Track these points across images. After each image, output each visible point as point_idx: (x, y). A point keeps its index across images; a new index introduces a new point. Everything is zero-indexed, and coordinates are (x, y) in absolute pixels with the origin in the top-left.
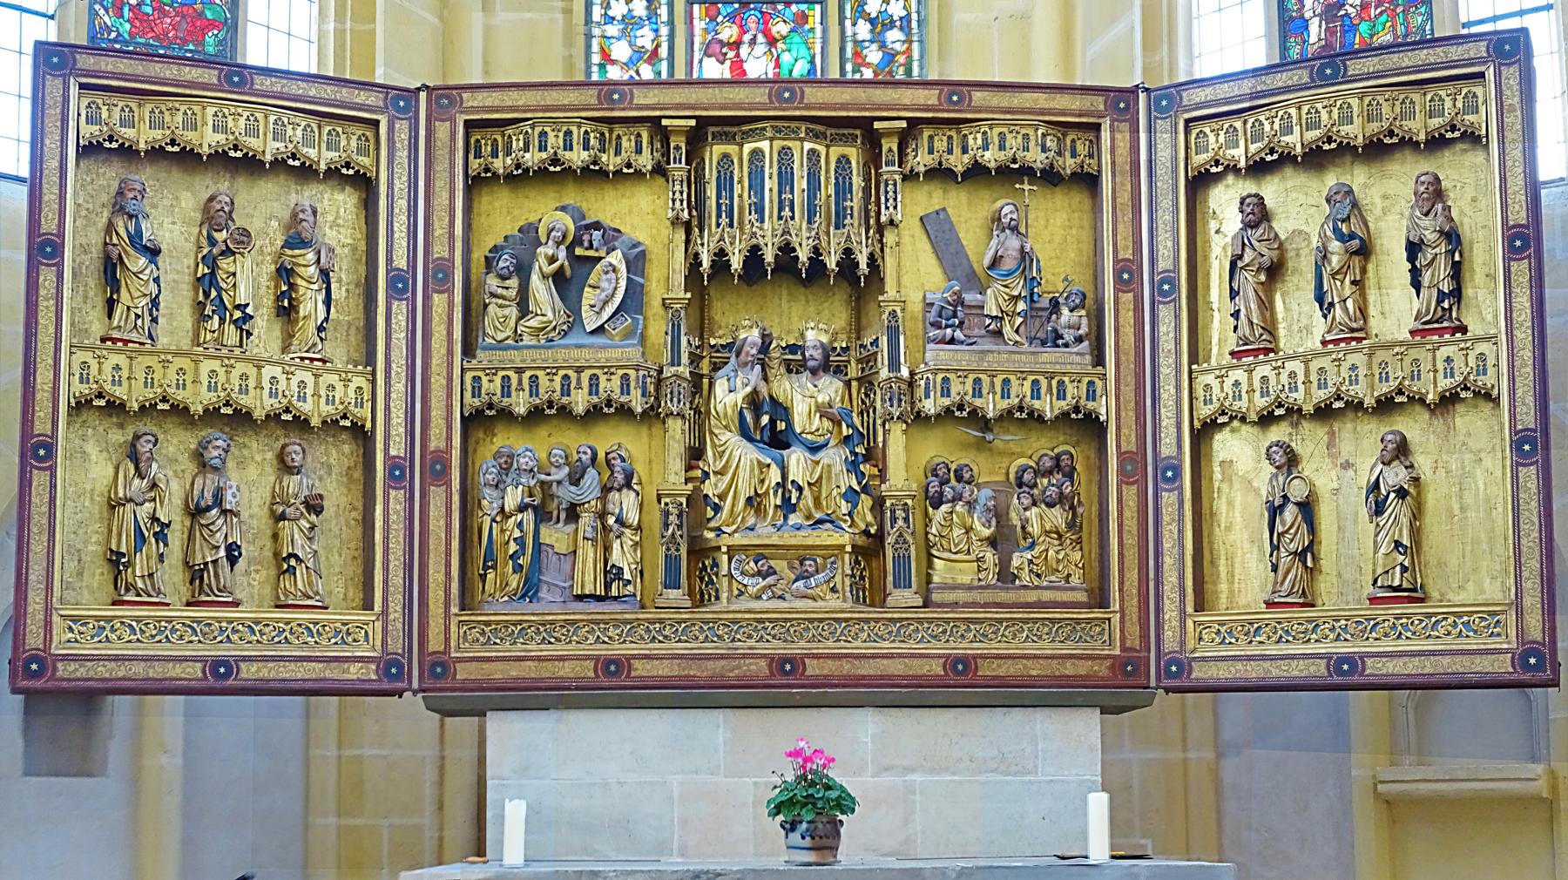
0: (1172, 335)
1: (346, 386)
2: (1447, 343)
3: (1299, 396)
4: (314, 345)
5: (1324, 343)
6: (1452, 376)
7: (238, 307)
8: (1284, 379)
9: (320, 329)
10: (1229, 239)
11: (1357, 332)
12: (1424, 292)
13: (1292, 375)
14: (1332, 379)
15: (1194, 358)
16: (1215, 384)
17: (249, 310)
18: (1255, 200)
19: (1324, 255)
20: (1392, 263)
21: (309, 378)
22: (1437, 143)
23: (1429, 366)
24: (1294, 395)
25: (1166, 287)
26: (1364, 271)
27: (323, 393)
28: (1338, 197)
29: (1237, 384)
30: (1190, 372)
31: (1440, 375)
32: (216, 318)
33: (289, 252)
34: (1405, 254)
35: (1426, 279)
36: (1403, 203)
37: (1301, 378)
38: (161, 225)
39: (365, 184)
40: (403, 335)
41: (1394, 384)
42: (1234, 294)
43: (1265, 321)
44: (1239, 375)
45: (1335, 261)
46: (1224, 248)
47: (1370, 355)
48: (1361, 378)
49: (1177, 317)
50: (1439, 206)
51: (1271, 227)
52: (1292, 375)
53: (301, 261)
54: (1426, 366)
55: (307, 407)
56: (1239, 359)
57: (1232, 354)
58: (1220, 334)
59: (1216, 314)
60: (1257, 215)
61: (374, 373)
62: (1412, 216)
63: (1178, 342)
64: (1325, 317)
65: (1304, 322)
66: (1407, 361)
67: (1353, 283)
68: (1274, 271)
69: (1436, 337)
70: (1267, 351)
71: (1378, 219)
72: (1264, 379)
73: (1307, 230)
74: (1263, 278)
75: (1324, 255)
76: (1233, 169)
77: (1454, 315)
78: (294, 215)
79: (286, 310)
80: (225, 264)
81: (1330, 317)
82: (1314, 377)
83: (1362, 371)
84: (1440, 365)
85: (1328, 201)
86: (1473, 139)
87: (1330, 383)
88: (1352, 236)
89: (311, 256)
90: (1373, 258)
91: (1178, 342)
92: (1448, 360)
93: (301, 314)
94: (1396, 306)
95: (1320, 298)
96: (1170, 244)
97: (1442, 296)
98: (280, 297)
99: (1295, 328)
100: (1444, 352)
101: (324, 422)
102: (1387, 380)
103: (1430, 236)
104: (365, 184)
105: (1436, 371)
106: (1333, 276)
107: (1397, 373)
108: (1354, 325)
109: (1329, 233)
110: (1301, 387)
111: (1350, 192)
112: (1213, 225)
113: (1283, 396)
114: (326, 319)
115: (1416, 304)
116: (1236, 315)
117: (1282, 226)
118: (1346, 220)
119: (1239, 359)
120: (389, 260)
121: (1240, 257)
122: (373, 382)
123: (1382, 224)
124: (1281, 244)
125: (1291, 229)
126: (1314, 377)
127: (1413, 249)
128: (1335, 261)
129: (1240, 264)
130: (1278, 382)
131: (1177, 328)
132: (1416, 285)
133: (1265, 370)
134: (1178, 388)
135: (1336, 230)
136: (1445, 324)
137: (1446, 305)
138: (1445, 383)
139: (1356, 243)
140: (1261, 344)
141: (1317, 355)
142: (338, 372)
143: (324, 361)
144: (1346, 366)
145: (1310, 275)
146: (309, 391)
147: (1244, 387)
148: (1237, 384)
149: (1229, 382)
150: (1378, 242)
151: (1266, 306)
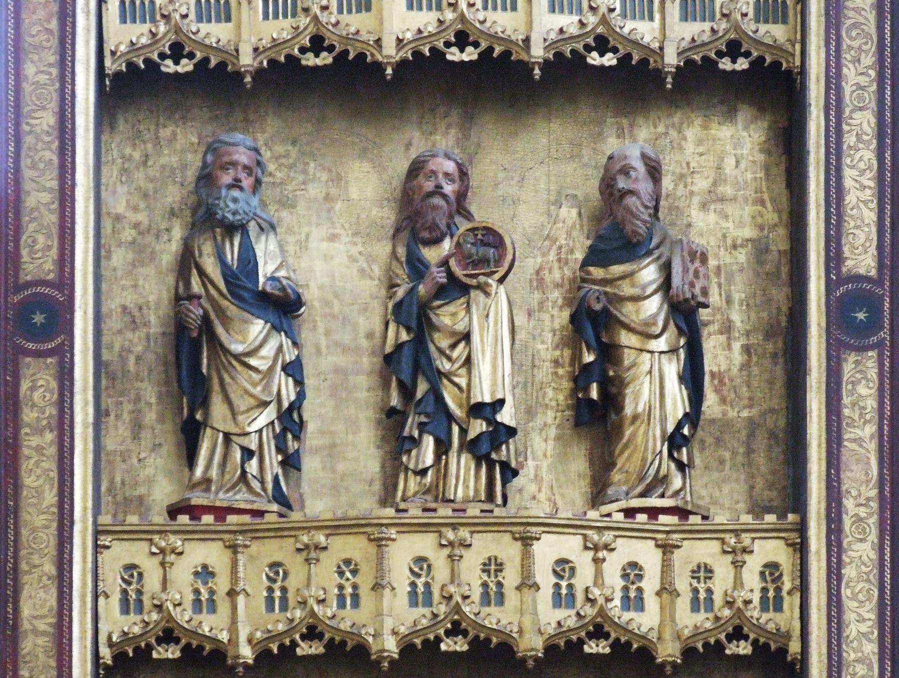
1: (738, 565)
4: (661, 480)
7: (477, 410)
9: (675, 441)
17: (506, 416)
21: (647, 555)
27: (683, 584)
32: (429, 442)
33: (597, 272)
38: (303, 245)
39: (771, 89)
40: (870, 429)
53: (626, 289)
55: (646, 621)
61: (802, 528)
78: (608, 186)
79: (597, 413)
80: (449, 316)
89: (649, 274)
93: (628, 410)
98: (581, 377)
101: (688, 652)
104: (771, 89)
114: (693, 416)
120: (834, 257)
122: (801, 548)
142: (717, 533)
143: (682, 513)
146: (650, 584)
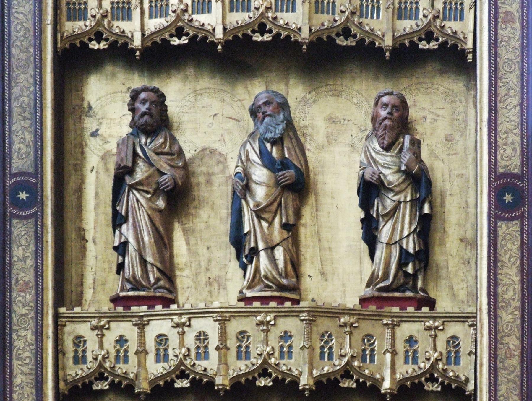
0: (30, 262)
2: (411, 319)
3: (211, 364)
5: (243, 299)
6: (415, 361)
8: (190, 340)
10: (113, 147)
11: (287, 289)
12: (380, 252)
13: (202, 337)
14: (257, 347)
15: (60, 300)
16: (91, 338)
18: (153, 96)
19: (244, 186)
20: (337, 210)
22: (404, 58)
23: (387, 345)
24: (204, 363)
25: (23, 196)
26: (298, 215)
28: (269, 110)
29: (121, 340)
30: (57, 316)
31: (400, 360)
34: (356, 199)
35: (385, 232)
36: (355, 131)
37: (214, 341)
41: (339, 363)
42: (118, 220)
43: (162, 260)
44: (126, 329)
45: (261, 193)
46: (104, 158)
47: (310, 323)
48: (296, 350)
49: (39, 238)
50: (407, 138)
51: (173, 140)
52: (202, 337)
54: (382, 343)
56: (127, 307)
57: (116, 300)
58: (99, 276)
59: (90, 245)
60: (153, 121)
62: (366, 151)
63: (39, 273)
64: (244, 268)
65: (215, 272)
66: (358, 335)
67: (285, 226)
68: (178, 198)
69: (396, 309)
70: (167, 302)
71: (320, 148)
72: (162, 339)
73: (222, 149)
74: (161, 203)
75: (244, 186)
76: (120, 53)
77: (420, 284)
81: (251, 269)
82: (232, 343)
83: (298, 342)
84: (401, 347)
85: (254, 112)
86: (456, 60)
87: (254, 352)
88: (285, 164)
90: (312, 199)
91: (39, 273)
92: (411, 340)
94: (340, 264)
95: (238, 239)
96: (29, 137)
97: (405, 257)
99: (203, 278)
100: (407, 329)
102: (330, 357)
103: (391, 177)
105: (394, 353)
106: (259, 213)
107: (345, 348)
108: (284, 281)
109: (254, 157)
110: (214, 355)
111: (284, 106)
112: (90, 124)
113: (188, 362)
115: (368, 268)
116: (122, 249)
117: (190, 141)
118: (277, 142)
119: (127, 307)
121: (131, 171)
123: (326, 156)
124: (186, 166)
125: (200, 145)
126: (232, 343)
127: (370, 190)
128: (261, 193)
129: (129, 180)
130: (182, 344)
131: (39, 254)
132: (370, 238)
133: (158, 327)
134: (39, 334)
135: (264, 154)
136: (409, 294)
137: (410, 269)
138: (406, 370)
139: (290, 173)
140: (152, 290)
141: (237, 314)
144: (275, 333)
145: (224, 210)
147: (133, 346)
148: (121, 340)
149: (110, 338)
150: (320, 179)
151: (164, 242)
